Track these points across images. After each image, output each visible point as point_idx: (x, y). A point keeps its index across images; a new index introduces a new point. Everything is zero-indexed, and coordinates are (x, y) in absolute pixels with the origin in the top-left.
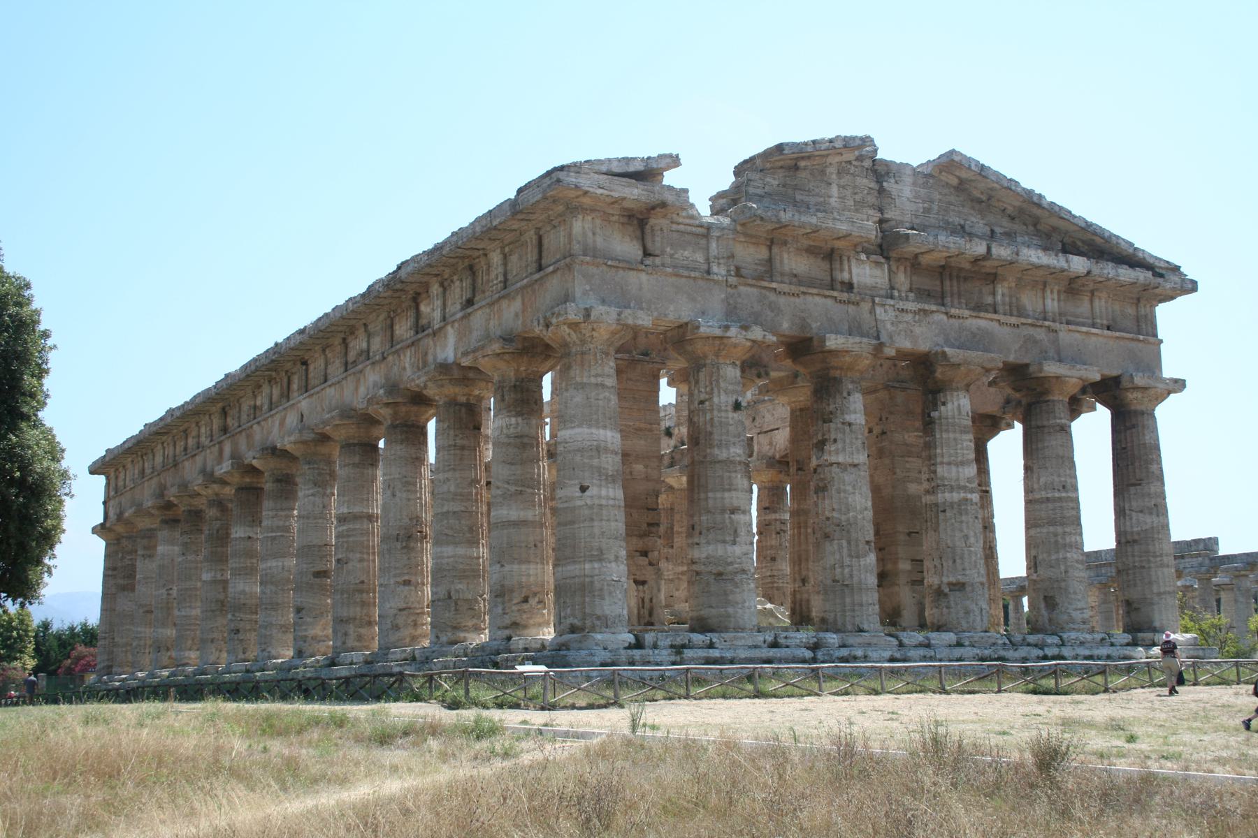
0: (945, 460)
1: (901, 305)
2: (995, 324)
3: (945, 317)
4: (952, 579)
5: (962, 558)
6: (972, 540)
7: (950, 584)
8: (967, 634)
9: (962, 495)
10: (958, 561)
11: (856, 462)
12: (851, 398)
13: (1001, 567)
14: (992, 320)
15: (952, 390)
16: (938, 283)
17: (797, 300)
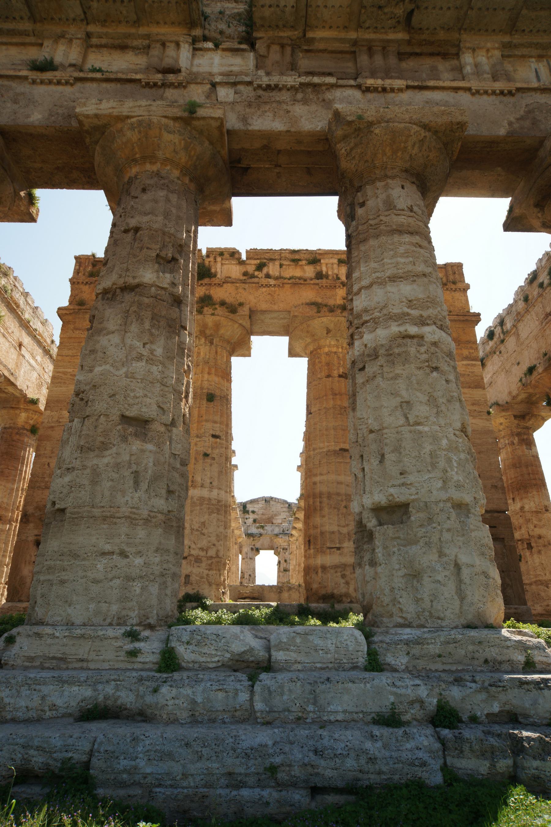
0: (364, 283)
1: (266, 81)
2: (464, 98)
3: (357, 94)
4: (379, 497)
5: (397, 450)
6: (421, 410)
7: (377, 510)
8: (407, 633)
9: (395, 329)
10: (390, 457)
11: (132, 281)
12: (145, 197)
13: (306, 366)
14: (456, 89)
15: (373, 182)
16: (350, 64)
17: (68, 89)
